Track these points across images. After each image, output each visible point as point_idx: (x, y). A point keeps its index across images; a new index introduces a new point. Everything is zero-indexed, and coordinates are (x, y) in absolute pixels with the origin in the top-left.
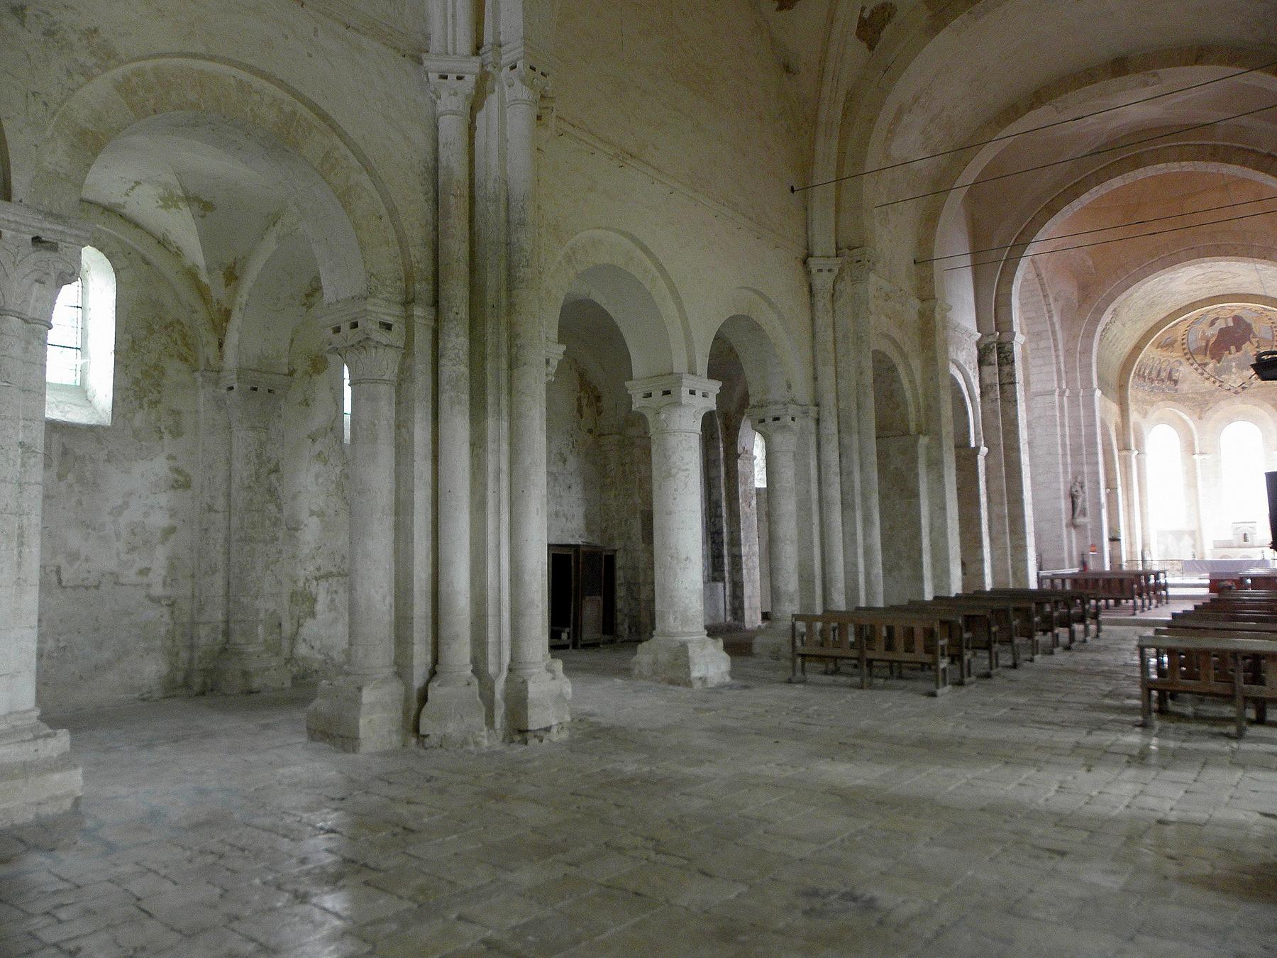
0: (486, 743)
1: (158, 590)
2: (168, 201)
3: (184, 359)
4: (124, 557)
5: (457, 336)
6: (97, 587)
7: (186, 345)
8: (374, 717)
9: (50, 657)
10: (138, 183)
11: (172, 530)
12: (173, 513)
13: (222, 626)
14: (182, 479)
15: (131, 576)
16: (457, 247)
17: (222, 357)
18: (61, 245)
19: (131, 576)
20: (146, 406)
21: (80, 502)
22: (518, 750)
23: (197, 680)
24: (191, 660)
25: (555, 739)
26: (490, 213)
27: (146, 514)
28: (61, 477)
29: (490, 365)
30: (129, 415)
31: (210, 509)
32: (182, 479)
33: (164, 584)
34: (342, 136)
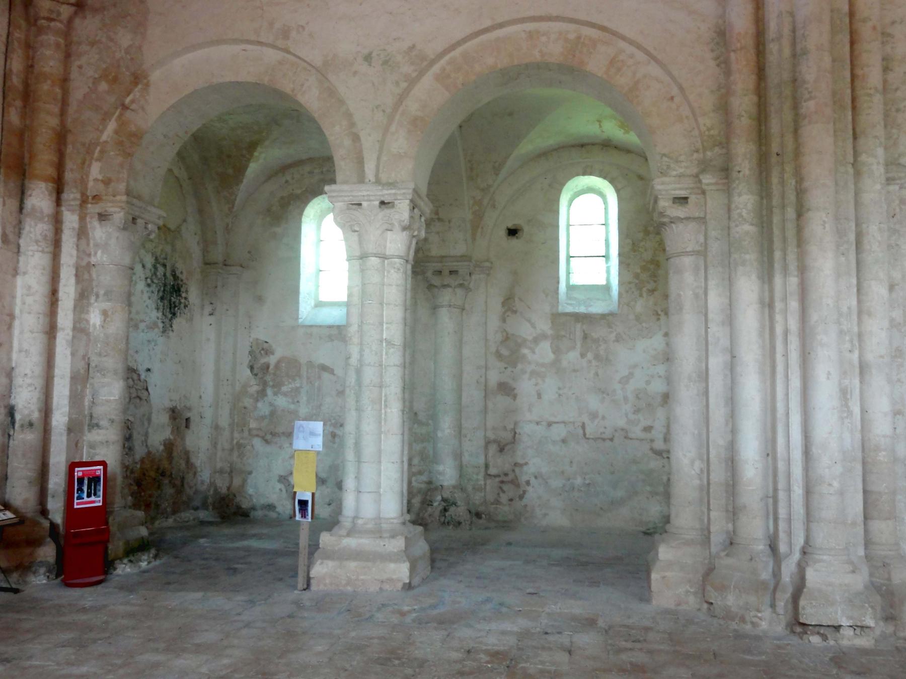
0: (764, 625)
4: (632, 417)
5: (740, 195)
6: (611, 440)
8: (667, 574)
9: (579, 490)
10: (599, 121)
15: (637, 432)
16: (743, 103)
18: (396, 202)
20: (645, 295)
21: (597, 374)
22: (795, 640)
25: (845, 643)
26: (778, 53)
27: (648, 383)
28: (583, 355)
29: (776, 219)
30: (633, 303)
34: (623, 38)
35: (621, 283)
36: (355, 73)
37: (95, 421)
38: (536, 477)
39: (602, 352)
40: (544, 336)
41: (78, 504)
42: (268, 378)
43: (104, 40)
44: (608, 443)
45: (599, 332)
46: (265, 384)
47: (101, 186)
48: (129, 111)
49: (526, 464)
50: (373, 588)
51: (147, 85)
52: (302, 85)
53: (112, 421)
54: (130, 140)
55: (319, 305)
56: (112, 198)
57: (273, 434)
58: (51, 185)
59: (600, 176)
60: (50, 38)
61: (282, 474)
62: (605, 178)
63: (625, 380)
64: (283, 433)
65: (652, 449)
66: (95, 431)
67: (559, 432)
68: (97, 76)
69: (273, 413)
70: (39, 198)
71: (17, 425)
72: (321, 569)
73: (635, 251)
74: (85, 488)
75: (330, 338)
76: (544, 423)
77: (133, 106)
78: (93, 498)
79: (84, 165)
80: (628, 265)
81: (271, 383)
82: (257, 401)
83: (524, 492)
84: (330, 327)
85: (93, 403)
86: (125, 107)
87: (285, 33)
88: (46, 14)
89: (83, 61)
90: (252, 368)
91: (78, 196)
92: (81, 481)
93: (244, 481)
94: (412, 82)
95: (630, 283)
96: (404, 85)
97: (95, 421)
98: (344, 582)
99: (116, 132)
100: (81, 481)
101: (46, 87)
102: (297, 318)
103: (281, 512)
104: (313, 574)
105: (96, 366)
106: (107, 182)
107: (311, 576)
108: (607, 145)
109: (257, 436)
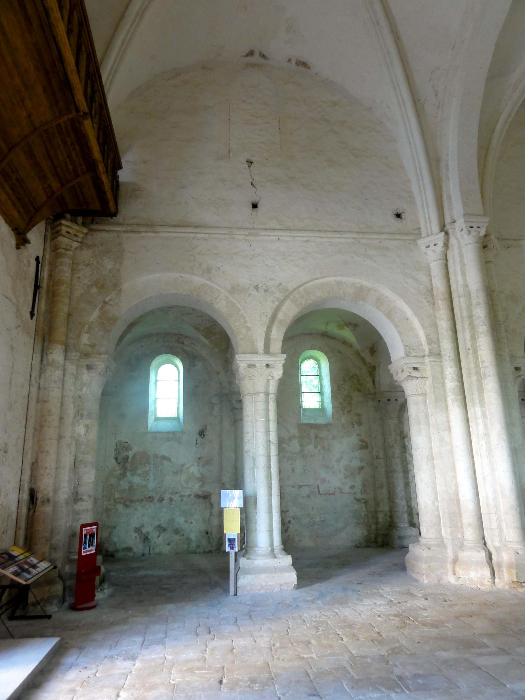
1: (359, 496)
2: (340, 327)
3: (359, 391)
6: (334, 494)
7: (360, 384)
8: (432, 564)
10: (328, 323)
11: (362, 468)
12: (362, 460)
13: (389, 514)
14: (364, 444)
17: (375, 387)
19: (347, 489)
20: (346, 414)
21: (324, 457)
23: (380, 540)
24: (377, 529)
28: (316, 447)
31: (377, 457)
32: (364, 444)
33: (361, 493)
35: (333, 407)
36: (249, 295)
37: (79, 497)
38: (294, 519)
39: (326, 445)
40: (294, 437)
41: (84, 552)
42: (128, 465)
43: (95, 263)
44: (332, 496)
45: (323, 434)
46: (125, 469)
47: (89, 349)
48: (108, 305)
49: (288, 511)
50: (276, 590)
51: (120, 291)
52: (216, 298)
53: (90, 496)
54: (107, 321)
55: (157, 419)
56: (97, 356)
57: (131, 501)
58: (64, 347)
59: (319, 350)
60: (67, 261)
61: (137, 526)
62: (322, 351)
63: (339, 460)
64: (138, 500)
65: (355, 498)
66: (79, 504)
67: (305, 491)
68: (90, 284)
69: (131, 488)
70: (57, 354)
71: (39, 502)
72: (244, 581)
73: (339, 390)
74: (87, 541)
75: (169, 440)
76: (297, 486)
77: (111, 303)
78: (91, 548)
79: (79, 336)
80: (336, 398)
81: (129, 468)
82: (120, 480)
83: (288, 528)
84: (168, 433)
85: (78, 484)
86: (105, 303)
87: (209, 270)
88: (65, 247)
89: (81, 274)
90: (116, 459)
91: (78, 354)
92: (86, 536)
93: (111, 533)
94: (282, 303)
95: (338, 407)
96: (277, 303)
97: (79, 497)
98: (259, 588)
99: (99, 317)
100: (86, 536)
101: (63, 288)
102: (147, 428)
103: (136, 552)
104: (239, 584)
105: (81, 461)
106: (93, 346)
107: (238, 586)
108: (325, 335)
109: (120, 503)
